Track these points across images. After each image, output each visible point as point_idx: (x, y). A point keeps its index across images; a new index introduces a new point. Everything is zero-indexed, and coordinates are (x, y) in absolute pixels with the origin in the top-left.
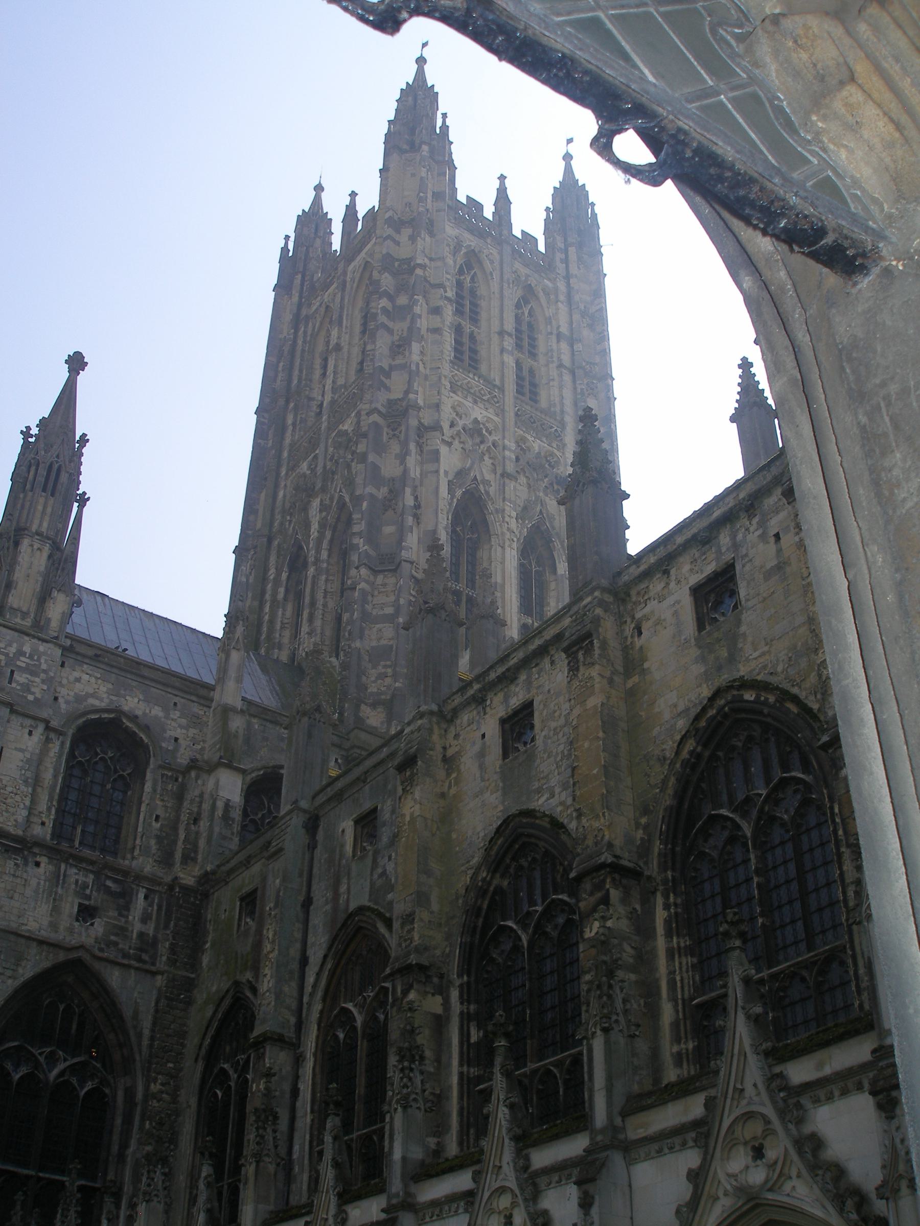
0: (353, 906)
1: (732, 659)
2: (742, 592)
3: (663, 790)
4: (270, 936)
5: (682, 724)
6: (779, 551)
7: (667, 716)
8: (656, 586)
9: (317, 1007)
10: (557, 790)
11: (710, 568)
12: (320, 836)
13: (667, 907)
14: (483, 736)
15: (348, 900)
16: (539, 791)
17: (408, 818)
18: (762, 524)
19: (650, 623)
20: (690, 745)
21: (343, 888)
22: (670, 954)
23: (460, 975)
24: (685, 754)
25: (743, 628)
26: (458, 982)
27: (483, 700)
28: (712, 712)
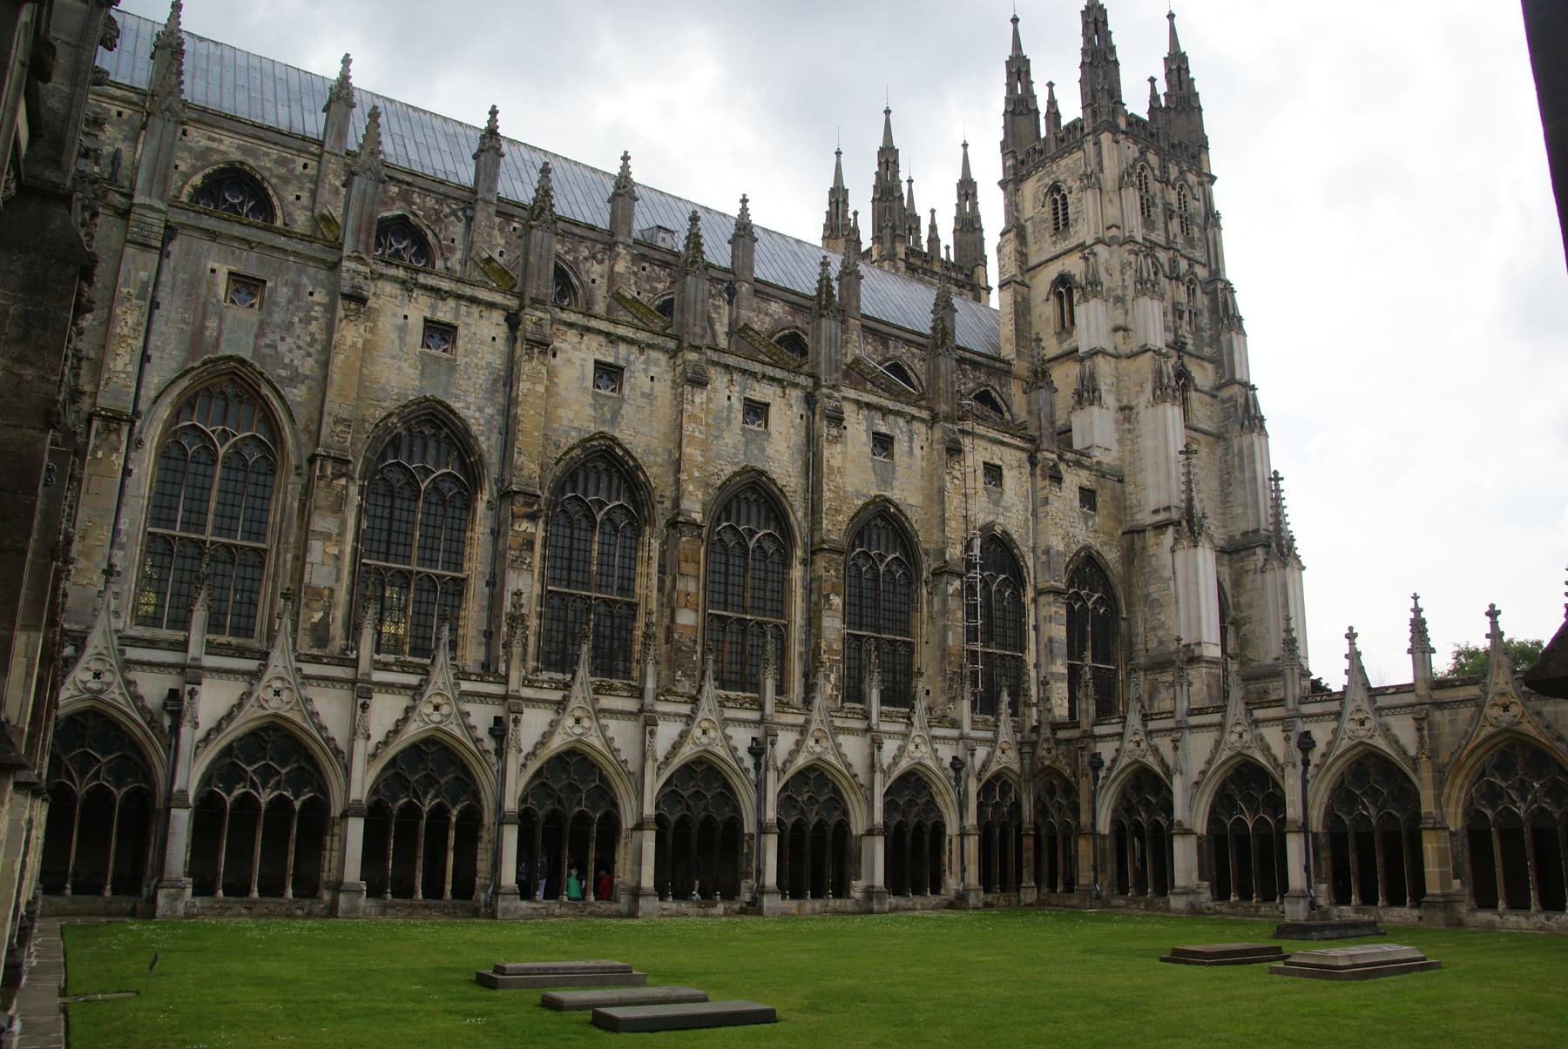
0: (225, 350)
1: (614, 421)
2: (626, 390)
3: (557, 464)
4: (130, 322)
5: (574, 438)
6: (652, 388)
7: (565, 422)
8: (572, 335)
9: (164, 411)
10: (472, 407)
11: (610, 360)
12: (175, 247)
13: (546, 531)
14: (406, 317)
15: (218, 339)
16: (457, 397)
17: (349, 343)
18: (647, 362)
19: (564, 356)
20: (578, 451)
21: (212, 324)
22: (544, 557)
23: (362, 478)
24: (573, 454)
25: (623, 412)
26: (359, 482)
27: (412, 291)
28: (594, 443)
